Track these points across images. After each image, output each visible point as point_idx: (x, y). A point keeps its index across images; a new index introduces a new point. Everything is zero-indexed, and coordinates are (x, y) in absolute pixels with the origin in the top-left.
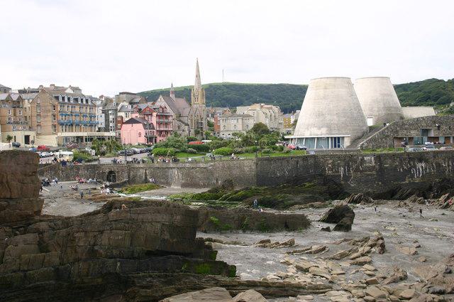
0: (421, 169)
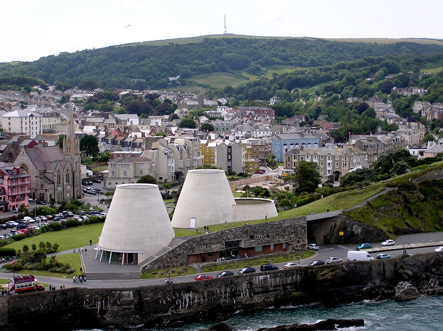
0: (188, 300)
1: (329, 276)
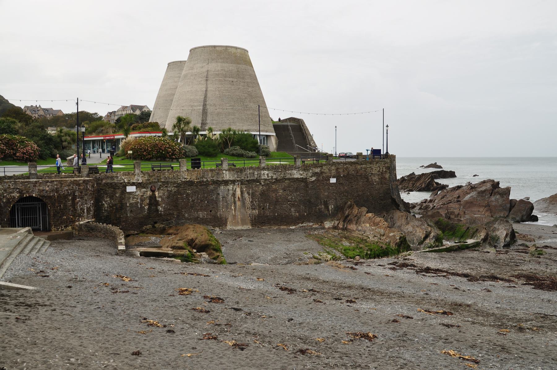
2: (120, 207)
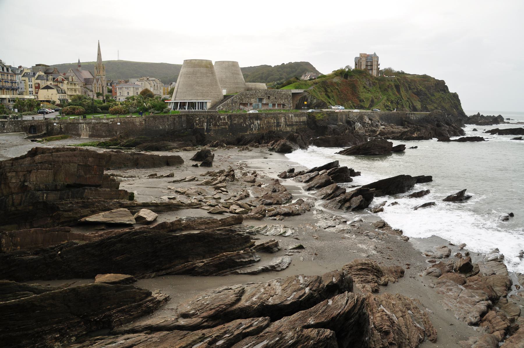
1: (321, 118)
2: (52, 129)
